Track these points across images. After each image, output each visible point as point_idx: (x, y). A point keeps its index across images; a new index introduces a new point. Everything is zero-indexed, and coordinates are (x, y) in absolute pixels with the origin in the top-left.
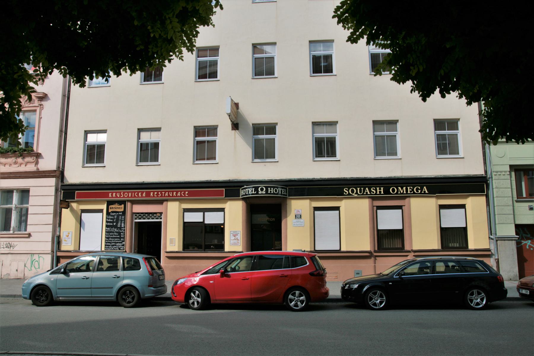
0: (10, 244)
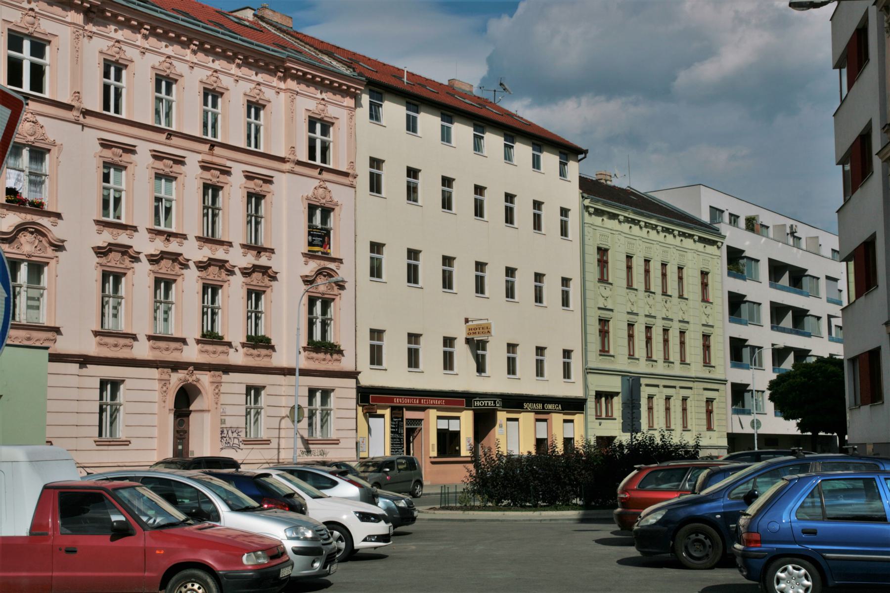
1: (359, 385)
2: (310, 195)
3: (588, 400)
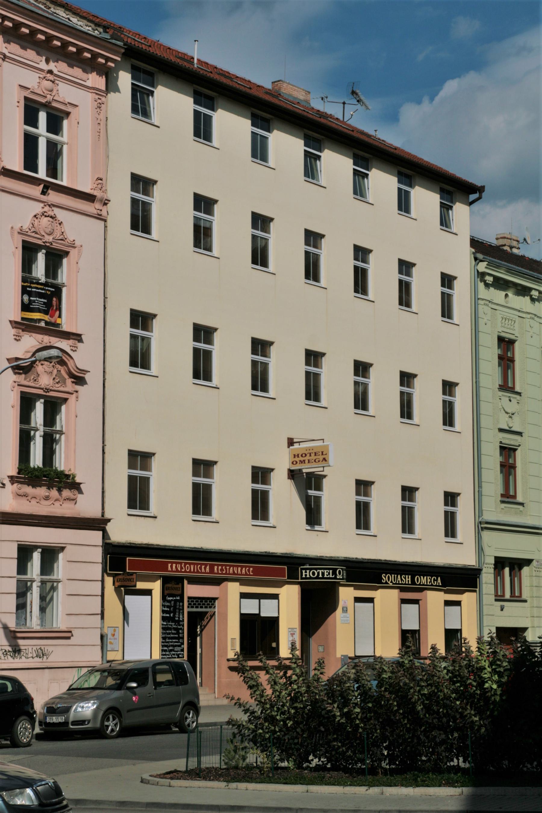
0: (42, 650)
1: (108, 541)
2: (26, 227)
3: (484, 570)
